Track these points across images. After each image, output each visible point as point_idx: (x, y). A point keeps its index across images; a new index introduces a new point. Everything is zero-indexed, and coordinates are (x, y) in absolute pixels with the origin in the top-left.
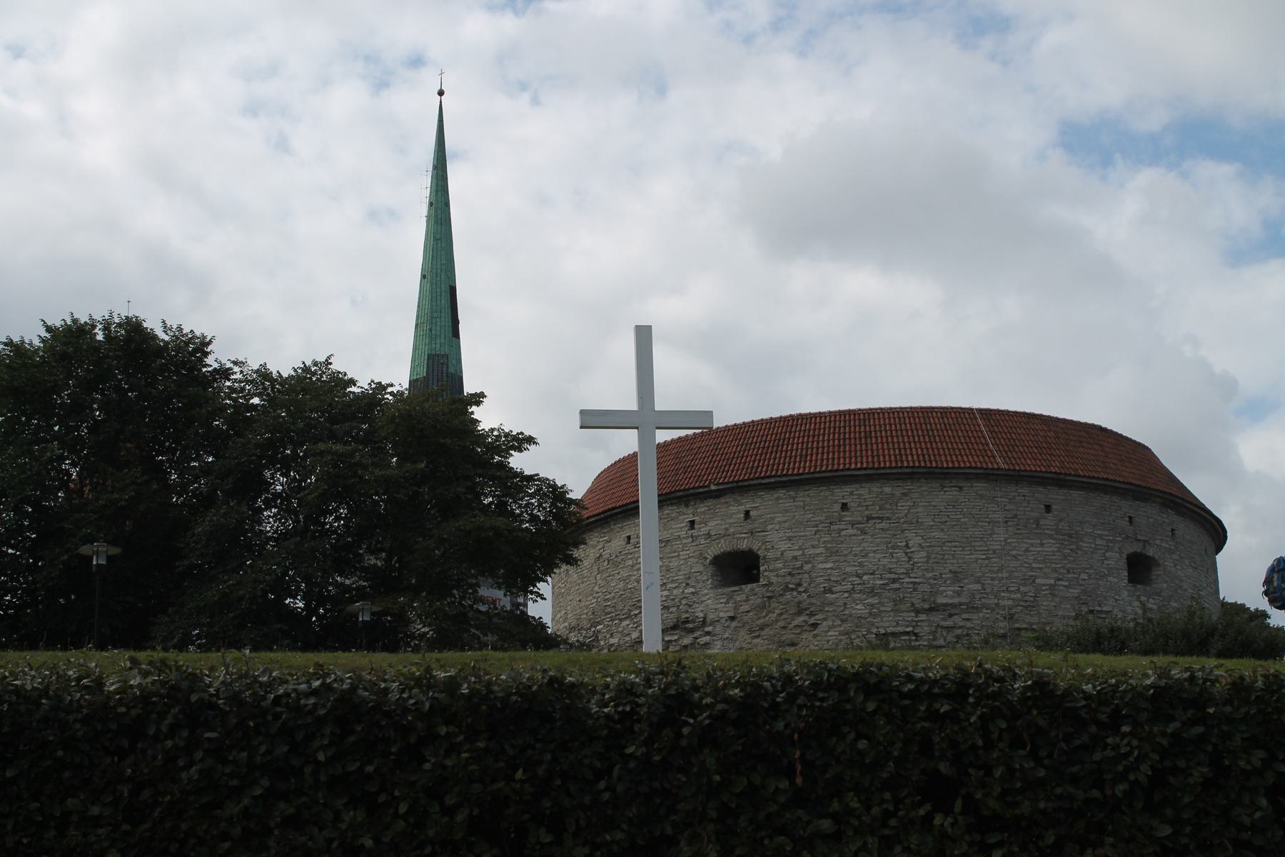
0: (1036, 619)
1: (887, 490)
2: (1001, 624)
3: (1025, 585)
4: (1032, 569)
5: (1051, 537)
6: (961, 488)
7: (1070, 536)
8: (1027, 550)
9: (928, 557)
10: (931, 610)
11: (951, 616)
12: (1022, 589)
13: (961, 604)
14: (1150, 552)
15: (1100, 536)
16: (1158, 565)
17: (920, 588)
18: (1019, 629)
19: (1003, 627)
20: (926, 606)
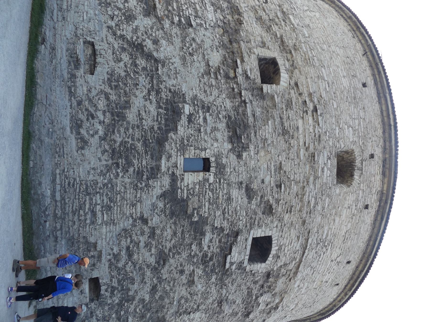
0: (300, 63)
1: (334, 12)
2: (290, 41)
3: (318, 60)
4: (328, 67)
5: (350, 83)
6: (354, 37)
7: (355, 98)
8: (338, 67)
9: (311, 17)
10: (283, 13)
11: (284, 21)
12: (315, 58)
13: (293, 25)
14: (356, 177)
15: (359, 124)
16: (349, 186)
17: (293, 10)
18: (291, 52)
19: (290, 43)
20: (285, 10)
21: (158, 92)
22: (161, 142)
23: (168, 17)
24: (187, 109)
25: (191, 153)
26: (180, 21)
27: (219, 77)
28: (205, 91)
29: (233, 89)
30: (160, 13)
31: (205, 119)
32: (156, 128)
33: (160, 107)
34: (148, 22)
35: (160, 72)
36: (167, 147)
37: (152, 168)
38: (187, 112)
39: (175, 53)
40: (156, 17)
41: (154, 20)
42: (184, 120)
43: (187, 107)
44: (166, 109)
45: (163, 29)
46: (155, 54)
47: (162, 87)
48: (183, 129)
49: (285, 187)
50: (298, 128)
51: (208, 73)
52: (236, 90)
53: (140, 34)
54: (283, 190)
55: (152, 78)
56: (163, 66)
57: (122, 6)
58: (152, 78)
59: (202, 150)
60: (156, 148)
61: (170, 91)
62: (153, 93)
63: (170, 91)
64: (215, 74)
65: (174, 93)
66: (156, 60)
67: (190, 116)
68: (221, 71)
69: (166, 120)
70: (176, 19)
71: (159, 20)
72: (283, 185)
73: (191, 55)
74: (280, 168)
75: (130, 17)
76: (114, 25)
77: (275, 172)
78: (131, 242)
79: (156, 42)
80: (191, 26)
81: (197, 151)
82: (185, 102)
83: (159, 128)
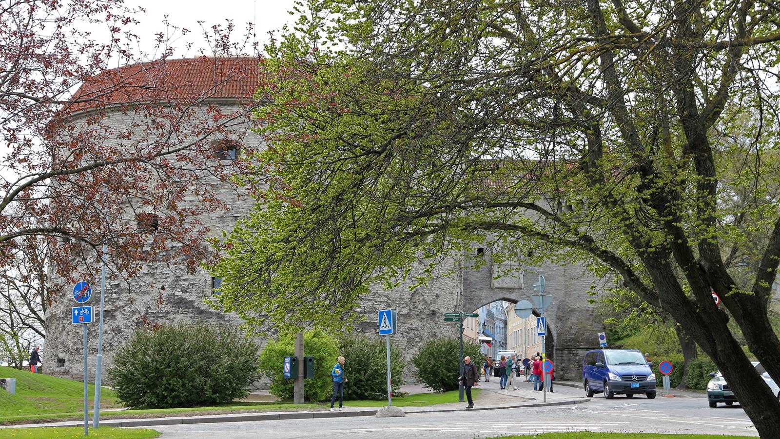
21: (168, 313)
22: (201, 312)
23: (114, 302)
24: (178, 293)
25: (208, 290)
26: (116, 293)
27: (155, 266)
28: (166, 278)
29: (163, 255)
30: (112, 308)
31: (185, 280)
32: (192, 315)
33: (178, 312)
34: (119, 316)
35: (155, 311)
36: (203, 308)
37: (218, 318)
38: (180, 293)
39: (141, 299)
40: (115, 311)
41: (118, 313)
42: (185, 296)
43: (177, 293)
44: (179, 307)
45: (123, 307)
46: (142, 314)
47: (164, 310)
48: (191, 297)
49: (236, 213)
50: (191, 201)
51: (153, 275)
52: (164, 254)
53: (129, 324)
54: (238, 215)
55: (159, 317)
56: (150, 309)
57: (110, 336)
58: (159, 317)
59: (206, 283)
60: (204, 315)
61: (167, 304)
62: (169, 316)
63: (167, 304)
64: (153, 269)
65: (169, 301)
66: (147, 314)
67: (182, 291)
68: (151, 264)
69: (186, 308)
70: (115, 296)
71: (117, 309)
72: (235, 215)
73: (140, 287)
74: (222, 217)
75: (118, 330)
76: (124, 341)
77: (224, 222)
78: (269, 331)
79: (134, 312)
80: (119, 284)
81: (207, 286)
82: (174, 294)
83: (192, 313)
